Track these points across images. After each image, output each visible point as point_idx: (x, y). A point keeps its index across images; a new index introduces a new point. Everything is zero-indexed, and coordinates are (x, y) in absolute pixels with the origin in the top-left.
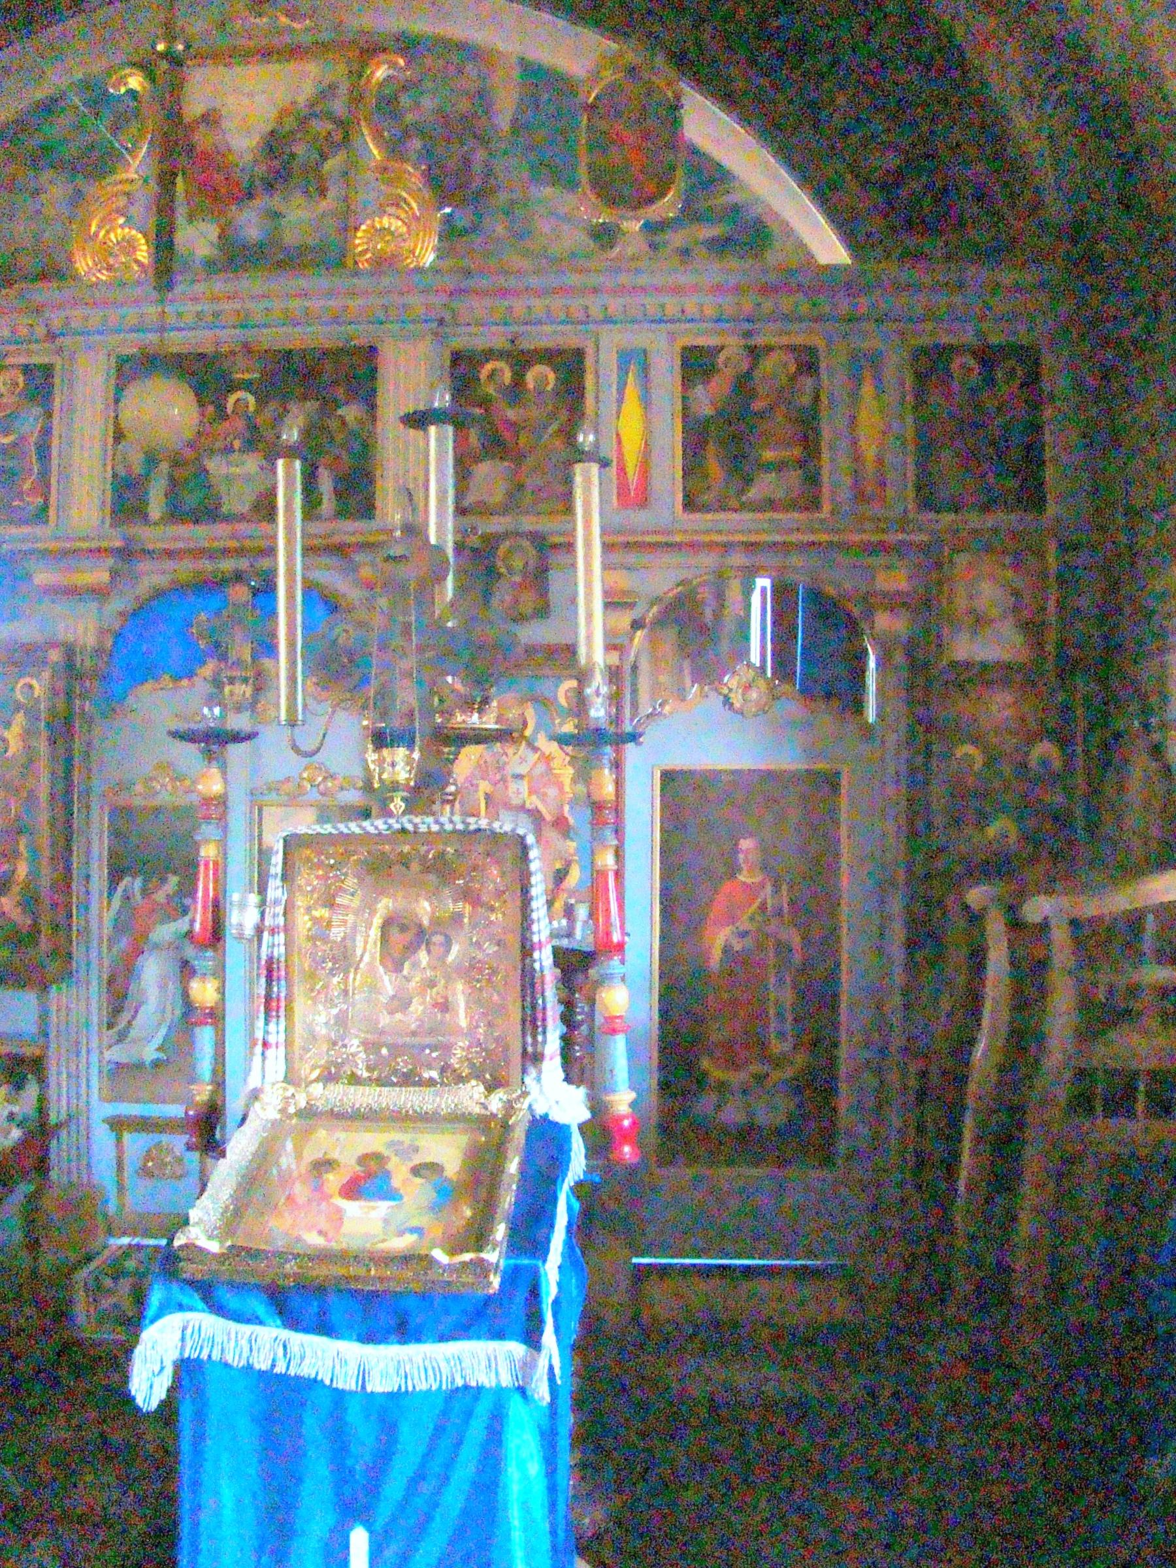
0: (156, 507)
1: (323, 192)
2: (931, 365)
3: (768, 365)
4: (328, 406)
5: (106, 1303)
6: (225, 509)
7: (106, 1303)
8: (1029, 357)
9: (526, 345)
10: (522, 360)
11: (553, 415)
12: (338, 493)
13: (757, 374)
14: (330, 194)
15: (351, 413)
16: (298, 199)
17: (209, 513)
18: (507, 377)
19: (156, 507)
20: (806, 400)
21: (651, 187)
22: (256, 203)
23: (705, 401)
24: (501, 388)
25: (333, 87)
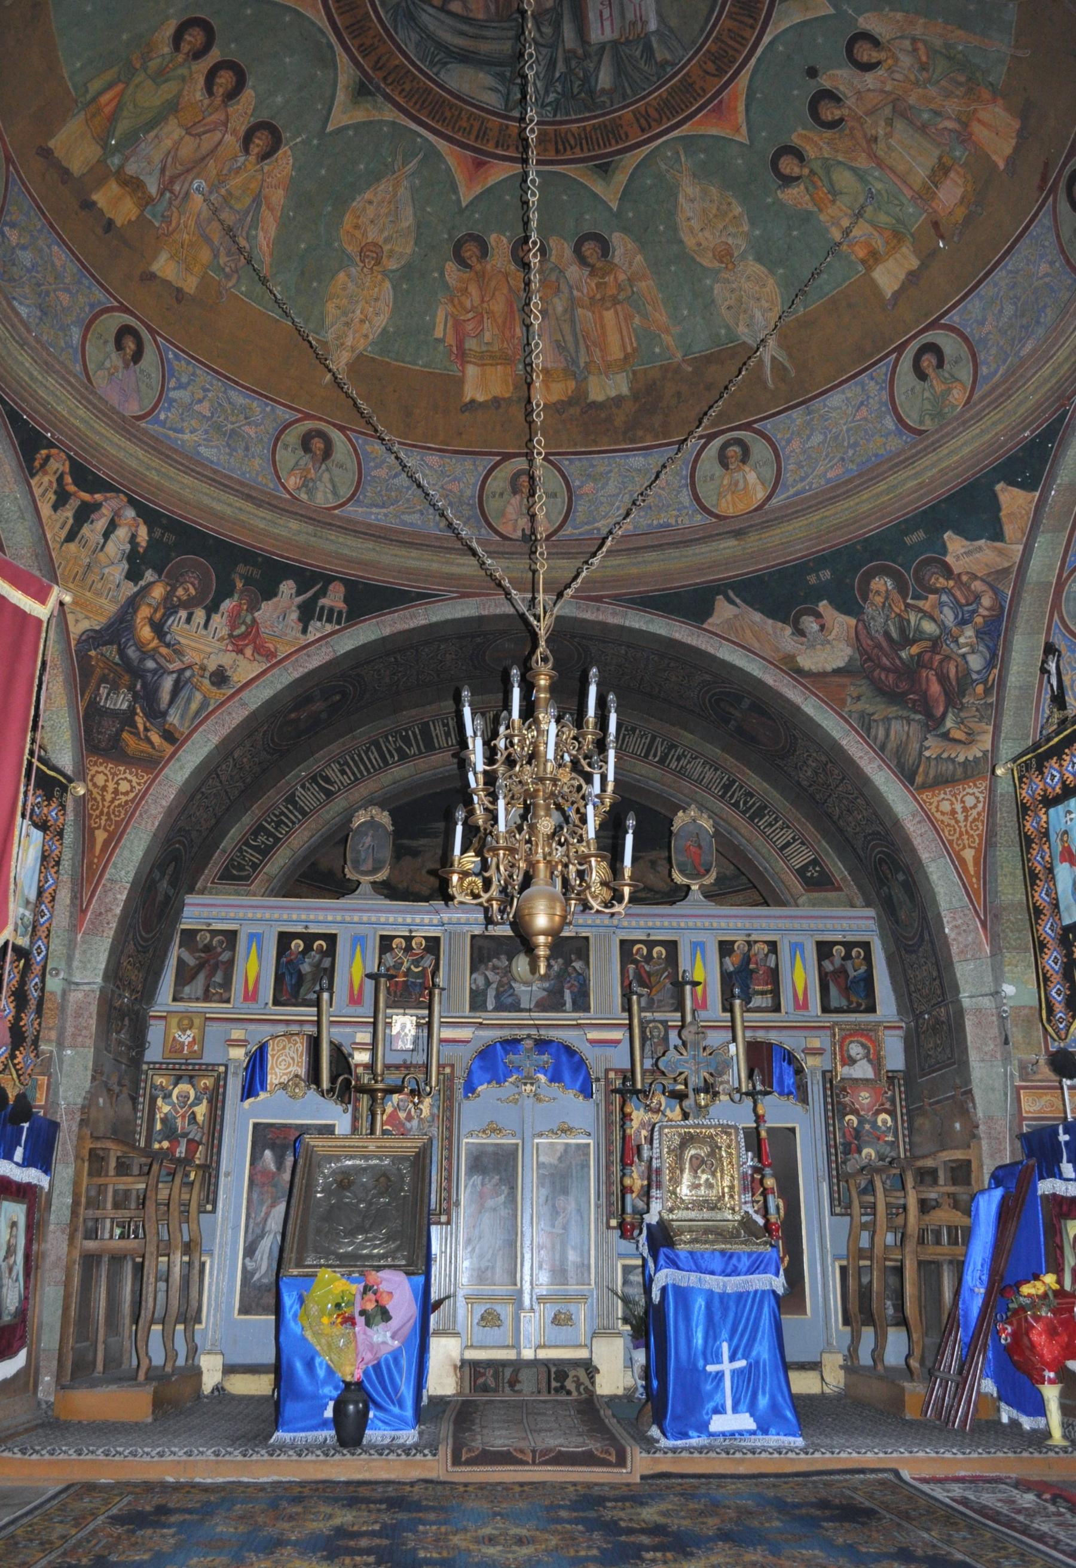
0: (491, 1004)
2: (824, 949)
3: (756, 947)
4: (568, 962)
5: (481, 1380)
7: (481, 1380)
8: (866, 946)
9: (652, 938)
10: (651, 944)
11: (665, 970)
12: (574, 1003)
13: (752, 952)
15: (578, 965)
17: (516, 1007)
18: (645, 952)
19: (491, 1004)
20: (773, 965)
21: (702, 870)
23: (730, 964)
24: (642, 956)
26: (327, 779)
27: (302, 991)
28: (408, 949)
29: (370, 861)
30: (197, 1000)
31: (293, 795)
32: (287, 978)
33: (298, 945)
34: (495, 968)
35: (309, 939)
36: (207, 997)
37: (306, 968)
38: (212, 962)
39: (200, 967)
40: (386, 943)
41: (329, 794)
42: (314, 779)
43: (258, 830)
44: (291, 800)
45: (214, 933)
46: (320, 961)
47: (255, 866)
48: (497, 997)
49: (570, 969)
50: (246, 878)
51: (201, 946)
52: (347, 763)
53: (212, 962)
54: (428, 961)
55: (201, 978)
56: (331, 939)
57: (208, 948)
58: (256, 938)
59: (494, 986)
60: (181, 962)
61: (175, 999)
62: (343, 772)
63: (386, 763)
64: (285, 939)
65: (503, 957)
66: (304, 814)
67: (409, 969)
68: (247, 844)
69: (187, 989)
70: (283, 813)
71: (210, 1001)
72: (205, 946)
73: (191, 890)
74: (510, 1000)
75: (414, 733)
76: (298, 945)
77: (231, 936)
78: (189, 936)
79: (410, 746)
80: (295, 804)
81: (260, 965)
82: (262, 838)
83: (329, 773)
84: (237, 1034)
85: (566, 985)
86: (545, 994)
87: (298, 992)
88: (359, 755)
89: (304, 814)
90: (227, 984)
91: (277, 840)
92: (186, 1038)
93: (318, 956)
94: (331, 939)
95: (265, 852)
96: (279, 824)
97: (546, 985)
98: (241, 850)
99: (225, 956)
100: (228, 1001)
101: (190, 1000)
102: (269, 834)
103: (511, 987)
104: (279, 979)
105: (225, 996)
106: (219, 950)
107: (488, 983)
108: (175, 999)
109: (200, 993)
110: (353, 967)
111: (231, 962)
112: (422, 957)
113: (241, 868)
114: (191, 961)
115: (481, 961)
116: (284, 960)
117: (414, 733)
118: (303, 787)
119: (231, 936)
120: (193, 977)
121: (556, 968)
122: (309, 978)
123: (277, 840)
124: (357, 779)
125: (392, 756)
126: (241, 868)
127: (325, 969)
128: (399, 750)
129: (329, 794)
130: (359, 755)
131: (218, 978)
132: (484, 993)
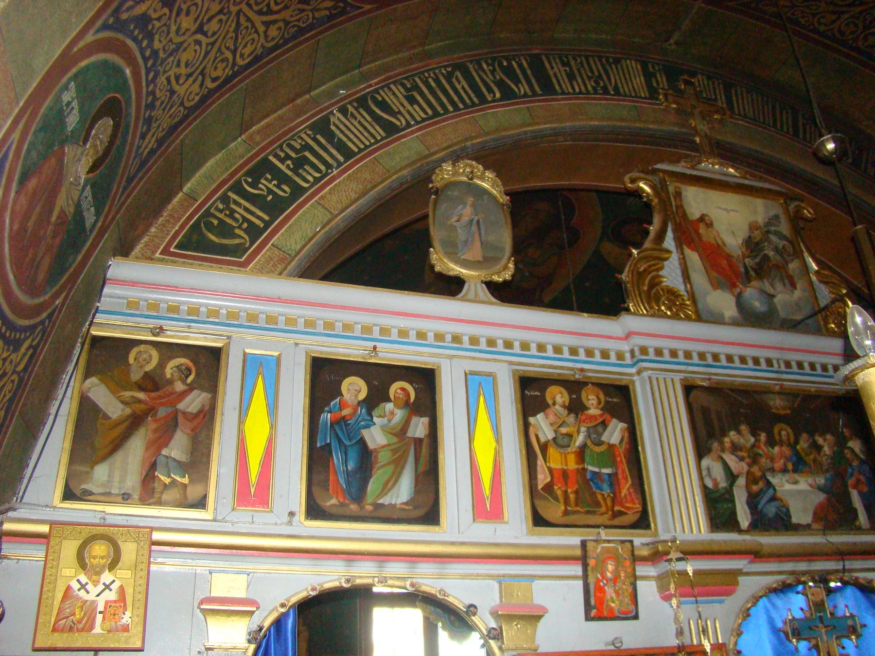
1: (793, 286)
6: (794, 520)
14: (798, 286)
16: (779, 286)
22: (754, 283)
25: (776, 217)
26: (384, 106)
27: (373, 486)
28: (576, 407)
29: (478, 244)
30: (126, 498)
31: (326, 121)
32: (337, 458)
33: (354, 389)
34: (735, 448)
35: (380, 377)
36: (149, 491)
37: (376, 437)
38: (162, 412)
39: (135, 422)
40: (531, 391)
41: (391, 129)
42: (362, 102)
43: (261, 169)
44: (323, 127)
45: (169, 350)
46: (406, 423)
47: (254, 232)
48: (753, 502)
49: (849, 455)
50: (238, 250)
51: (136, 376)
52: (416, 87)
53: (162, 412)
54: (615, 432)
55: (136, 448)
56: (425, 379)
57: (152, 382)
58: (266, 369)
59: (741, 481)
60: (87, 411)
61: (69, 495)
62: (412, 100)
63: (483, 100)
64: (325, 375)
65: (743, 428)
66: (348, 154)
67: (584, 447)
68: (238, 188)
69: (101, 471)
70: (307, 147)
71: (159, 503)
72: (147, 375)
73: (124, 250)
74: (771, 510)
75: (520, 66)
76: (354, 389)
77: (208, 362)
78: (109, 355)
79: (517, 82)
80: (330, 136)
81: (273, 426)
82: (267, 184)
83: (390, 99)
84: (229, 583)
85: (851, 482)
86: (822, 497)
87: (363, 489)
88: (437, 81)
89: (348, 154)
90: (198, 462)
91: (298, 191)
92: (97, 593)
93: (400, 415)
94: (425, 379)
95: (275, 208)
96: (300, 164)
97: (821, 480)
98: (225, 199)
99: (194, 402)
100: (201, 504)
101: (107, 497)
102: (282, 179)
103: (769, 484)
104: (317, 459)
105: (193, 493)
106: (179, 387)
107: (732, 477)
108: (69, 495)
109: (132, 482)
110: (479, 442)
111: (206, 418)
112: (604, 424)
113: (225, 230)
114: (113, 407)
115: (711, 435)
116: (326, 417)
117: (520, 66)
118: (343, 111)
119: (208, 362)
120: (117, 445)
121: (826, 449)
122: (383, 457)
123: (298, 191)
124: (436, 114)
125: (490, 91)
126: (225, 230)
127: (418, 442)
128: (501, 84)
129: (391, 129)
130: (437, 81)
131: (177, 448)
132: (727, 496)
